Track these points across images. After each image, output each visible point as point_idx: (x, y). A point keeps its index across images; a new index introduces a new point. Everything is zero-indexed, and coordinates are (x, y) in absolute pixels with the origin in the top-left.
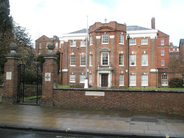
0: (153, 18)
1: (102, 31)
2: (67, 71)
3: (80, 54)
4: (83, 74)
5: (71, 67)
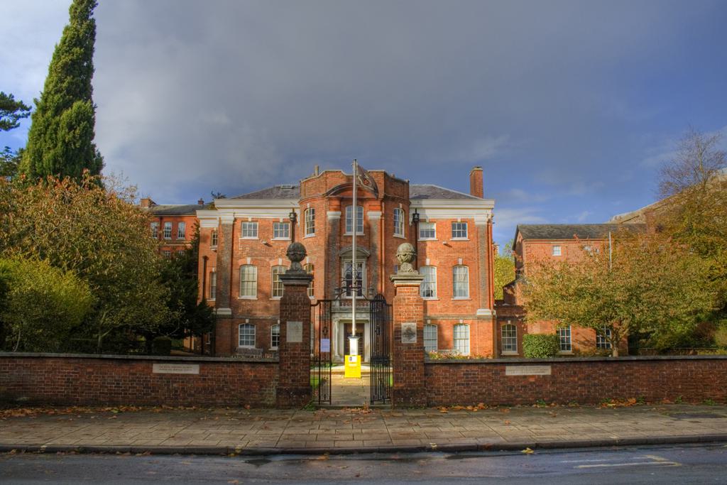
2: (230, 313)
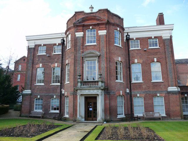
0: (160, 14)
1: (85, 24)
2: (30, 93)
3: (52, 66)
4: (55, 97)
5: (37, 87)
